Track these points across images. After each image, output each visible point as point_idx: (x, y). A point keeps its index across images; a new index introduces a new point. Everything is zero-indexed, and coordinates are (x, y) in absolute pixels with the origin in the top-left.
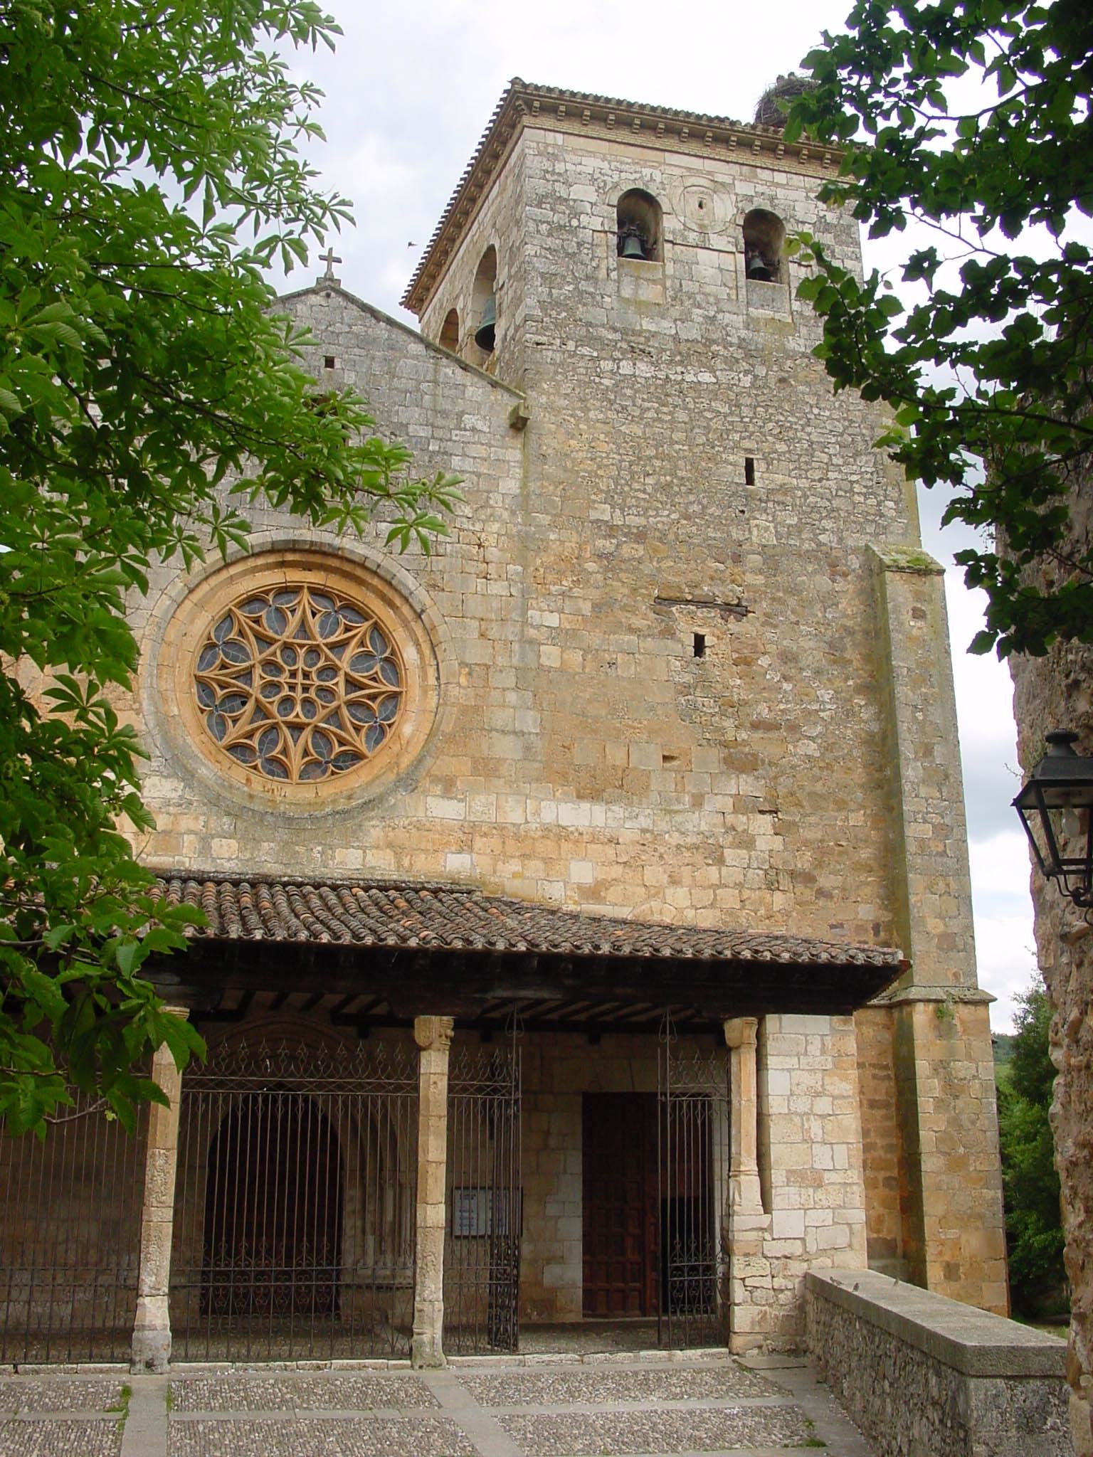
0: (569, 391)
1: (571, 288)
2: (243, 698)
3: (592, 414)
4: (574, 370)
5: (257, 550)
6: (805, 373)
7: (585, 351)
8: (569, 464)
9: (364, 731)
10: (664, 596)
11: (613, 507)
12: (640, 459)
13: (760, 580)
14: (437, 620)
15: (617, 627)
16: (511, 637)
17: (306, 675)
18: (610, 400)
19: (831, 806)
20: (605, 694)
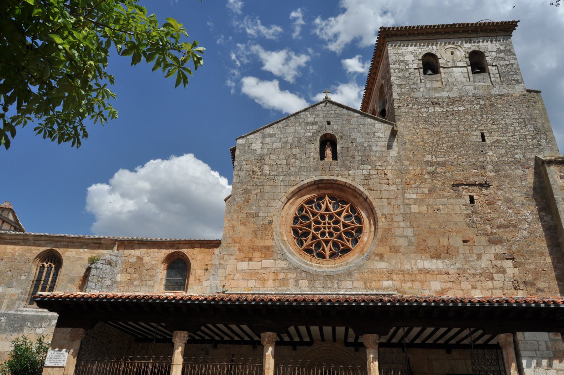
2: (308, 233)
3: (421, 127)
6: (500, 101)
7: (416, 106)
8: (414, 144)
9: (350, 241)
10: (455, 183)
11: (432, 156)
12: (440, 139)
15: (439, 196)
16: (399, 204)
17: (329, 224)
19: (537, 255)
20: (437, 220)
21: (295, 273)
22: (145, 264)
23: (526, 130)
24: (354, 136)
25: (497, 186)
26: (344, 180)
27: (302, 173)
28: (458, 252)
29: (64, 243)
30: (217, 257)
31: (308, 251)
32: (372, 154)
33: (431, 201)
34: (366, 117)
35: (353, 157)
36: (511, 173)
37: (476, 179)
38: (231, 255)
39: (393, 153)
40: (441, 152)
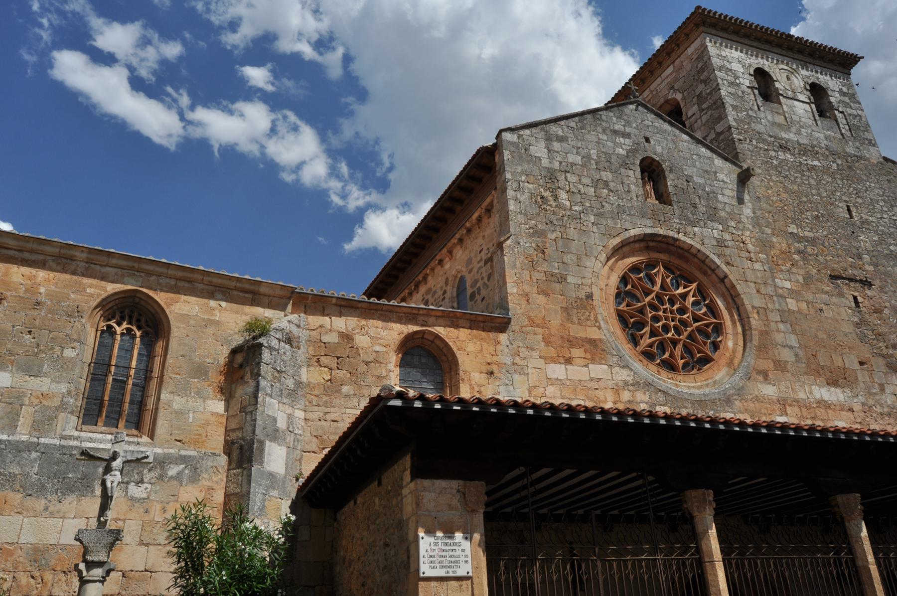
0: (760, 165)
1: (745, 113)
4: (759, 154)
5: (637, 238)
7: (761, 145)
10: (833, 274)
11: (797, 227)
12: (801, 202)
13: (871, 268)
14: (735, 282)
16: (771, 294)
18: (779, 172)
21: (647, 393)
22: (360, 351)
23: (893, 213)
24: (689, 172)
25: (880, 287)
26: (689, 241)
27: (624, 217)
28: (857, 379)
29: (168, 280)
30: (506, 350)
31: (648, 355)
32: (720, 206)
33: (810, 297)
34: (698, 143)
35: (694, 206)
36: (890, 271)
37: (855, 272)
38: (532, 349)
39: (747, 211)
40: (806, 223)
